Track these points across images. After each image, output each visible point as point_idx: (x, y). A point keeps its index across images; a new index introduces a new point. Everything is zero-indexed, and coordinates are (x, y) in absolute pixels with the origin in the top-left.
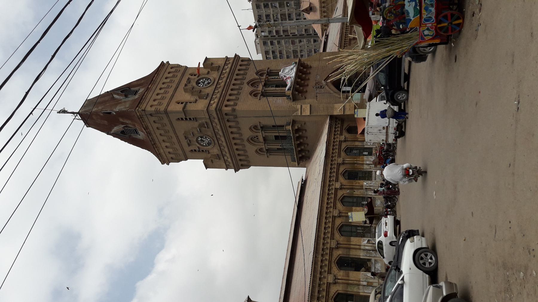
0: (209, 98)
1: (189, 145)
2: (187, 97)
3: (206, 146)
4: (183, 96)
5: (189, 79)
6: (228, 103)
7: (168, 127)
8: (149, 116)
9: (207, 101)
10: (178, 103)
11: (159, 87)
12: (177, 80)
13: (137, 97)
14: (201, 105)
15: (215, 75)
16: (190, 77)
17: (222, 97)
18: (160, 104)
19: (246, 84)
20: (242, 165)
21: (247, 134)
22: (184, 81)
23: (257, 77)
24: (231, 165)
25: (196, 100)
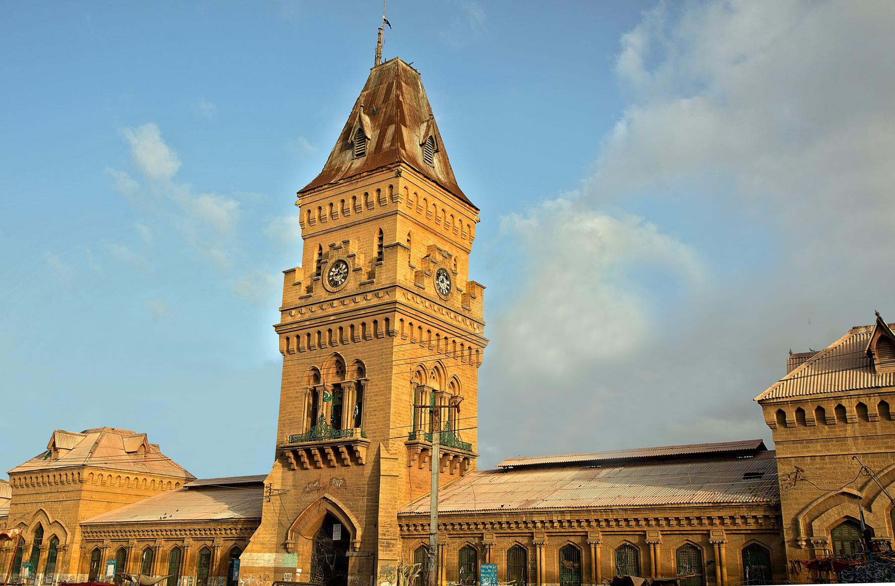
0: (415, 290)
1: (332, 246)
2: (418, 252)
3: (329, 276)
4: (421, 244)
5: (450, 256)
6: (406, 324)
7: (366, 214)
8: (389, 183)
9: (410, 285)
10: (409, 234)
11: (437, 202)
12: (450, 235)
13: (420, 161)
14: (403, 275)
15: (457, 301)
16: (453, 258)
17: (417, 314)
18: (410, 204)
19: (438, 357)
20: (288, 339)
21: (349, 356)
22: (447, 248)
23: (450, 374)
24: (289, 319)
25: (412, 268)
